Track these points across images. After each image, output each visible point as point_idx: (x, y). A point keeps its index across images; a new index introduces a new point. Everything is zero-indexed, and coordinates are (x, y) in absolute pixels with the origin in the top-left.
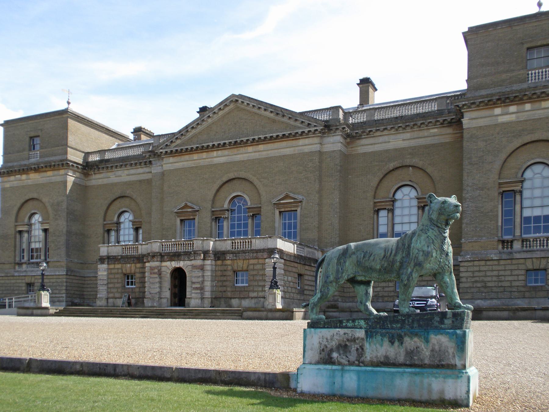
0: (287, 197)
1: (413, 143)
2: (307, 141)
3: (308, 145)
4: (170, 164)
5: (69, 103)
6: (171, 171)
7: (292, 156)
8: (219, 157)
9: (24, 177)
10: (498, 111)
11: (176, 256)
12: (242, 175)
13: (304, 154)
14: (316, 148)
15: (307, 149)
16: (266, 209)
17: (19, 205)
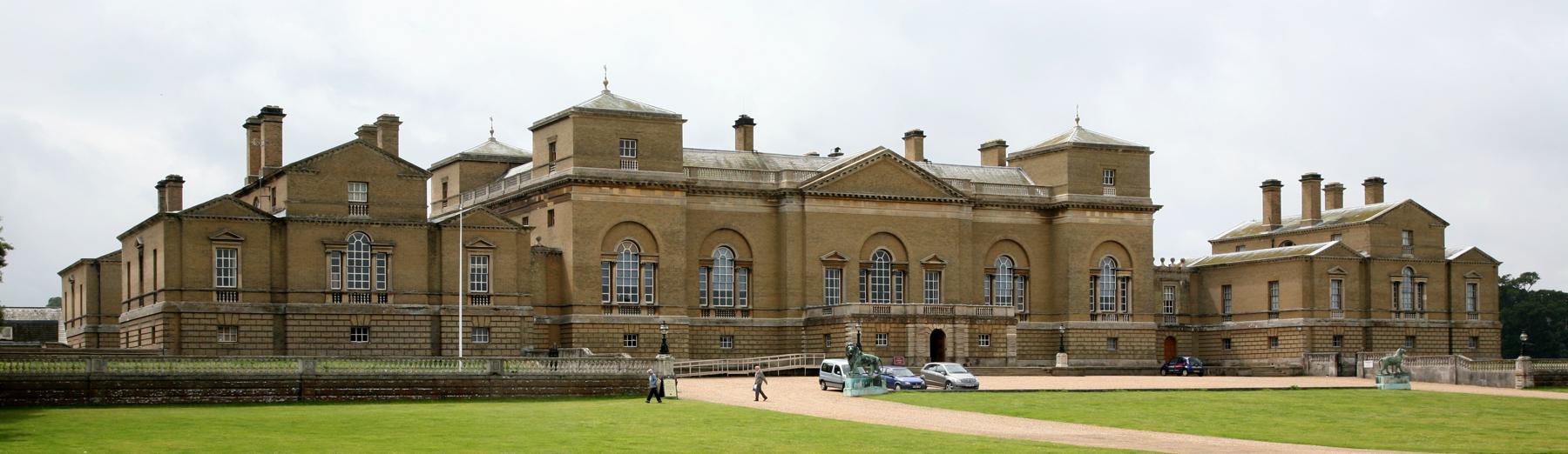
0: (935, 258)
1: (1014, 221)
2: (949, 208)
3: (949, 212)
4: (812, 206)
5: (606, 83)
6: (813, 214)
7: (936, 220)
8: (868, 209)
9: (616, 191)
10: (1088, 213)
11: (940, 319)
12: (891, 230)
13: (944, 219)
14: (954, 215)
15: (949, 215)
16: (914, 268)
17: (607, 227)
